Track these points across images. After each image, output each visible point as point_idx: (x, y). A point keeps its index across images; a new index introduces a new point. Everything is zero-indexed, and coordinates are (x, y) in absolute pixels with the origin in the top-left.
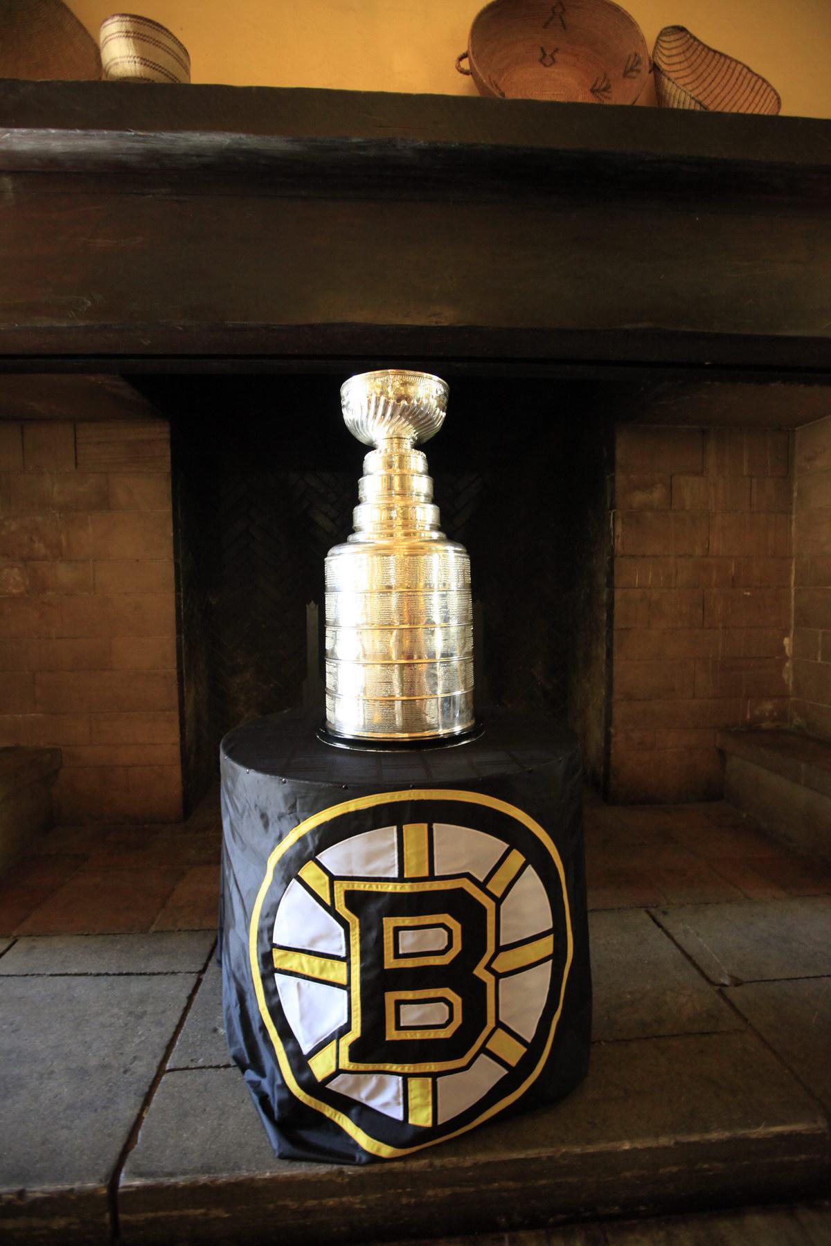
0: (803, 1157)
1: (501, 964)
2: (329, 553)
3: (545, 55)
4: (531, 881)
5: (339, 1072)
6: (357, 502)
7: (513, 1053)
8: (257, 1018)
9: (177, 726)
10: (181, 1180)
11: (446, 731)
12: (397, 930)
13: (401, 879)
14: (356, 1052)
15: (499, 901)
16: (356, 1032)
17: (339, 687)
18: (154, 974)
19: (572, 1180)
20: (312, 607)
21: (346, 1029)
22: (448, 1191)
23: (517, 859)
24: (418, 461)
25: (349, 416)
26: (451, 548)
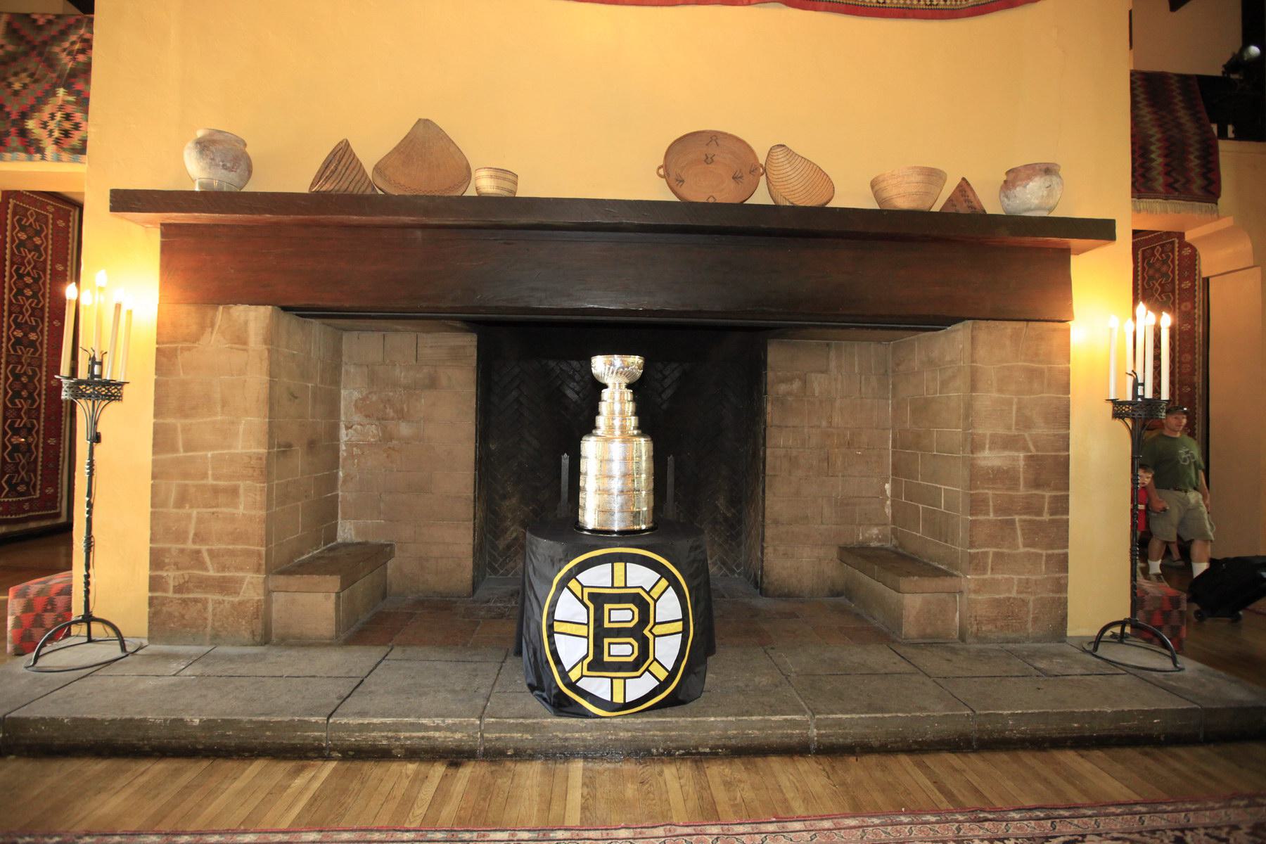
0: (797, 731)
1: (657, 630)
2: (584, 438)
3: (707, 158)
4: (671, 593)
5: (582, 676)
6: (598, 413)
7: (663, 675)
8: (544, 658)
9: (472, 535)
10: (512, 721)
11: (638, 527)
12: (610, 610)
13: (613, 587)
14: (590, 667)
15: (655, 601)
16: (590, 658)
17: (587, 504)
18: (476, 662)
19: (688, 733)
20: (565, 459)
21: (587, 656)
22: (630, 734)
23: (664, 583)
24: (628, 395)
25: (594, 371)
26: (642, 440)
